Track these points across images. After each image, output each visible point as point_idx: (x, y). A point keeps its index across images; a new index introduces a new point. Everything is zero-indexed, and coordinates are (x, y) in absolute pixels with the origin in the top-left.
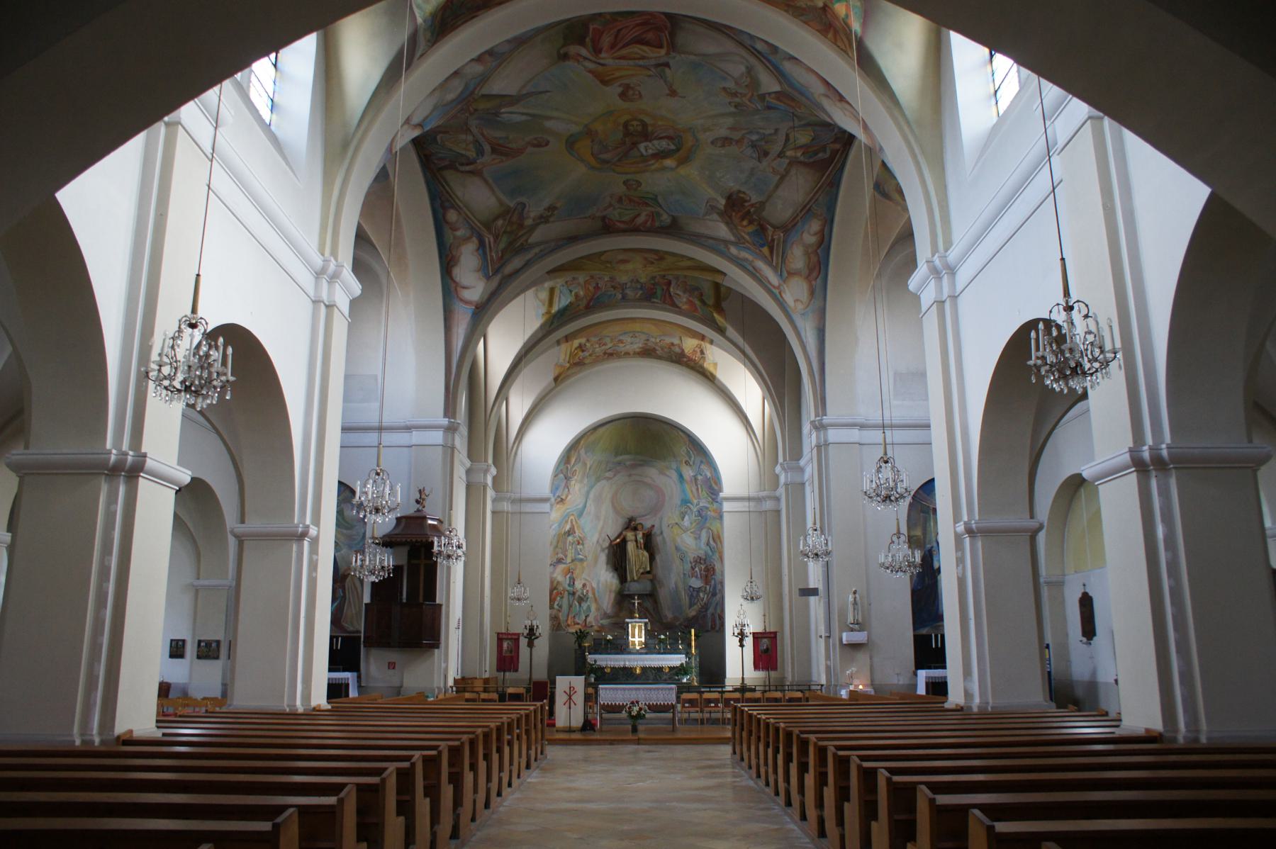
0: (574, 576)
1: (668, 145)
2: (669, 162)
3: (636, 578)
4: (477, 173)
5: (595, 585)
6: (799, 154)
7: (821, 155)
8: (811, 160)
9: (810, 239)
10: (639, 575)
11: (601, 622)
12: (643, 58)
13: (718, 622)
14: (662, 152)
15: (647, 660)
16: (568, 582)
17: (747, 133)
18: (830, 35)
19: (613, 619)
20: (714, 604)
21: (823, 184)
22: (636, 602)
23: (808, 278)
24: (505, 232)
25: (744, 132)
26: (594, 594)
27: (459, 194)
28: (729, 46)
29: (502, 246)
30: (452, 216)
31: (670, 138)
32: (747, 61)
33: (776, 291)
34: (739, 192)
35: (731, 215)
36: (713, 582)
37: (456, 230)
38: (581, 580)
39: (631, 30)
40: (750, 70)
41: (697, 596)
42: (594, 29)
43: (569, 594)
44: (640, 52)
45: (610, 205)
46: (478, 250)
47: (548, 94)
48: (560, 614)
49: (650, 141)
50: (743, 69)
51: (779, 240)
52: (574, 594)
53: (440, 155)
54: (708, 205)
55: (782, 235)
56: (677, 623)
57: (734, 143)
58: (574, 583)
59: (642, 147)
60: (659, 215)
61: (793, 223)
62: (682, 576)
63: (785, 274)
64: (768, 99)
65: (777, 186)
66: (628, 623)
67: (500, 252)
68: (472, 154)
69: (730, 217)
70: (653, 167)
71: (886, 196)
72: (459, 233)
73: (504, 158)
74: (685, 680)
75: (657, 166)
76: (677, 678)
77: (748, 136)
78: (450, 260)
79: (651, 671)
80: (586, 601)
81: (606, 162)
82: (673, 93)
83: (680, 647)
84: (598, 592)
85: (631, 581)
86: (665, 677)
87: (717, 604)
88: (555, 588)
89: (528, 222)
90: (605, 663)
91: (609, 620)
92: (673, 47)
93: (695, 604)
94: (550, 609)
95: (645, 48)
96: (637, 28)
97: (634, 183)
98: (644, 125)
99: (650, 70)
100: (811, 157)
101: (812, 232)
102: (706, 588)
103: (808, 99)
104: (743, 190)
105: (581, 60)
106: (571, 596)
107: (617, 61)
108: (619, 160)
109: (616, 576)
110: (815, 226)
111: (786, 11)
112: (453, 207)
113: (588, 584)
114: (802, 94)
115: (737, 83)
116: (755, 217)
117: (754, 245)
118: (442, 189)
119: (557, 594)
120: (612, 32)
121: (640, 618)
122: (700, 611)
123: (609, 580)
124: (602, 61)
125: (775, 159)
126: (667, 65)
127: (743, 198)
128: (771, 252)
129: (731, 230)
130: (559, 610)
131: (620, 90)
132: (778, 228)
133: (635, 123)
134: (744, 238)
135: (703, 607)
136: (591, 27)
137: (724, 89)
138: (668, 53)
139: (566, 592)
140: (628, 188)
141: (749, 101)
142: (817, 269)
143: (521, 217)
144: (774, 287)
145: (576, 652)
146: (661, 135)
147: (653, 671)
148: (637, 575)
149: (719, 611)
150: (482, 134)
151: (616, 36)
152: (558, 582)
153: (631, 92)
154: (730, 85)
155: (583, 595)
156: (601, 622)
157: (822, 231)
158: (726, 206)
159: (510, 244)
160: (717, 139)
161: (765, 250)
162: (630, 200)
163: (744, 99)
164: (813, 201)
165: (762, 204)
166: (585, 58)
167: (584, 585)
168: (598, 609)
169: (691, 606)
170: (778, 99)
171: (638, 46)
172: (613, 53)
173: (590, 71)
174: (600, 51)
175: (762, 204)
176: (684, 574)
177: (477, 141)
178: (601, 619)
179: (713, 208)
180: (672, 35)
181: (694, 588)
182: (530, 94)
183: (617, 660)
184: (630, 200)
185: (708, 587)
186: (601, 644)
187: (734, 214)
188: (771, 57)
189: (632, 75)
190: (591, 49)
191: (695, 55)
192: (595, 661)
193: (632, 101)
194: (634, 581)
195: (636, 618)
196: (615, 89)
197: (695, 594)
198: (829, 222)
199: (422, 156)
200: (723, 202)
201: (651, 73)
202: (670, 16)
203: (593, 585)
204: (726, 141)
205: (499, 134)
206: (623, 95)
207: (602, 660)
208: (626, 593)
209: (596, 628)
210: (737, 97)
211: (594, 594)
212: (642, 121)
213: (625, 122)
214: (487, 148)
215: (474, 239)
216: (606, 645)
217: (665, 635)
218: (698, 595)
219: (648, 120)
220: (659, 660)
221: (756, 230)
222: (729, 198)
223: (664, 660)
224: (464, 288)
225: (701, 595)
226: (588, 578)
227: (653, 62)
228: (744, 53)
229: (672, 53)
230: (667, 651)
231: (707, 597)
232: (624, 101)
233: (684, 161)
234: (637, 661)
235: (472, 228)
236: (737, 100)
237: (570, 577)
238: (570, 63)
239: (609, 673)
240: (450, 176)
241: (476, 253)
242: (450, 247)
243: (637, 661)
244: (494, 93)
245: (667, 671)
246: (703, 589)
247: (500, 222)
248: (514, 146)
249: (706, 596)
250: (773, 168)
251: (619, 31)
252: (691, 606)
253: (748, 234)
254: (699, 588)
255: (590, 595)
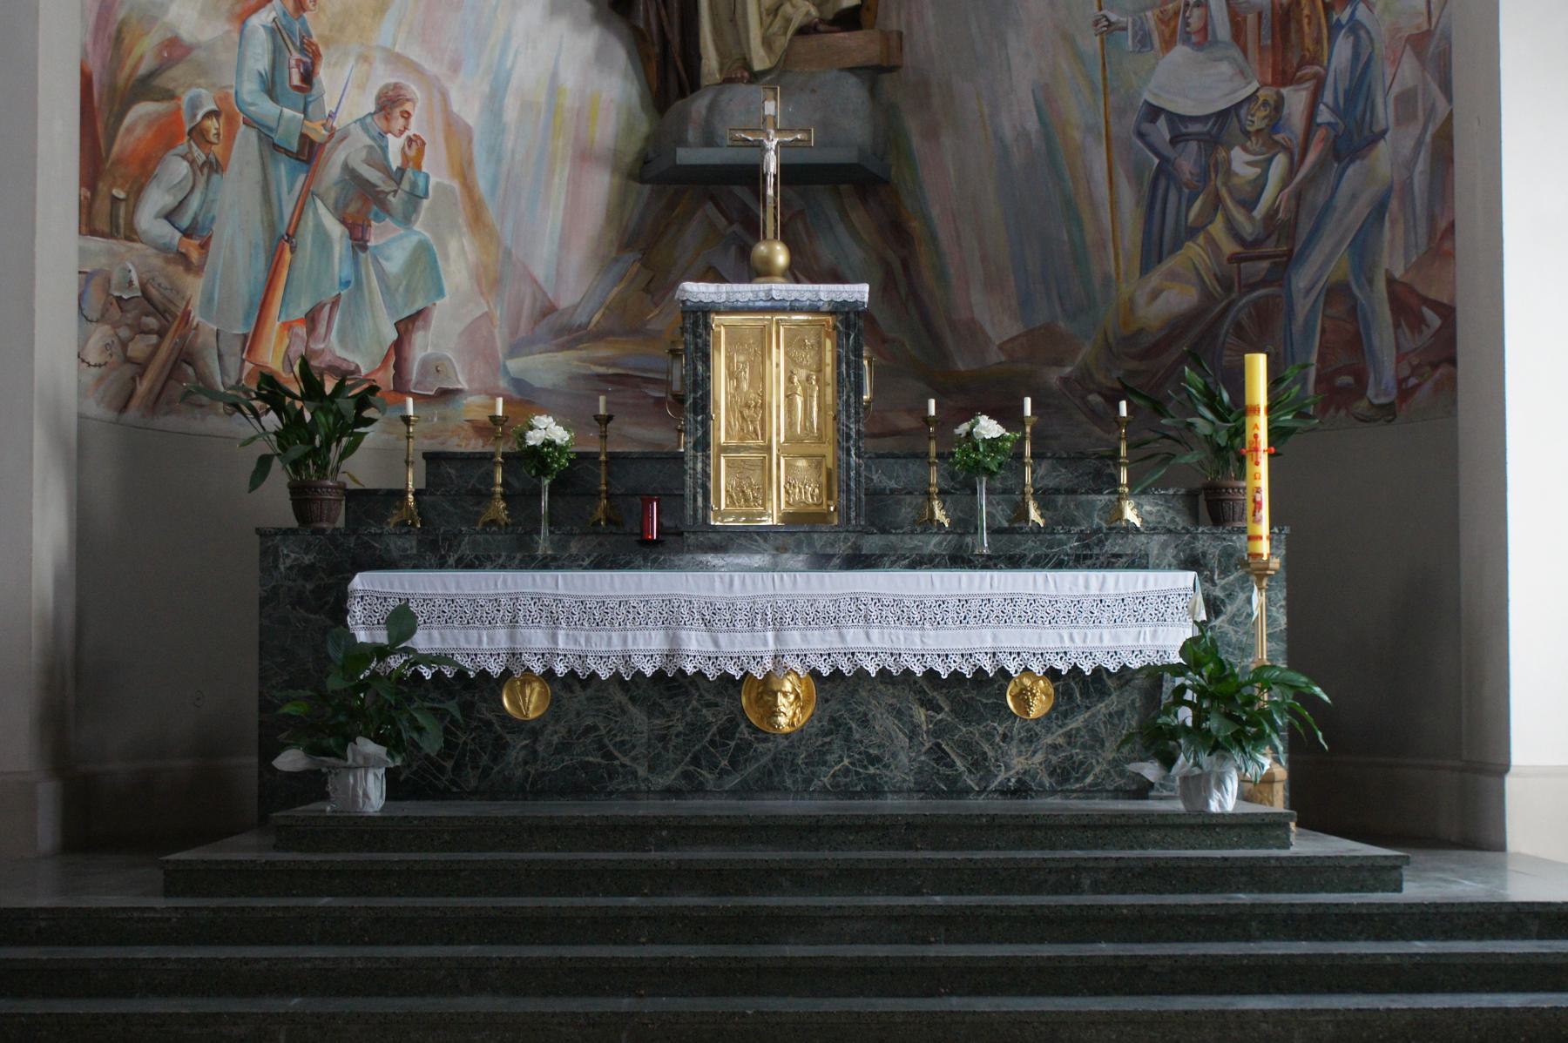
0: (317, 24)
3: (760, 60)
5: (469, 111)
10: (782, 43)
11: (514, 365)
13: (1384, 337)
15: (863, 612)
16: (259, 58)
19: (603, 352)
20: (1350, 215)
22: (772, 144)
26: (464, 172)
36: (1342, 51)
38: (364, 58)
41: (1204, 175)
43: (271, 146)
48: (195, 287)
52: (308, 153)
56: (1053, 377)
58: (308, 77)
62: (1091, 44)
66: (700, 315)
74: (1225, 800)
76: (1150, 771)
79: (899, 714)
80: (407, 220)
83: (1130, 514)
84: (495, 153)
85: (728, 80)
86: (1018, 762)
87: (1380, 209)
88: (144, 88)
90: (502, 639)
91: (561, 356)
93: (1192, 233)
94: (88, 226)
102: (1279, 103)
106: (283, 168)
109: (619, 54)
113: (414, 89)
119: (167, 135)
121: (796, 273)
122: (1226, 284)
123: (570, 79)
130: (183, 258)
135: (1249, 249)
139: (246, 143)
145: (269, 555)
147: (920, 715)
148: (767, 43)
149: (1394, 260)
152: (175, 50)
155: (385, 168)
156: (514, 365)
167: (390, 103)
168: (490, 280)
169: (1153, 252)
176: (1109, 29)
178: (514, 351)
181: (1175, 119)
183: (599, 615)
185: (1296, 100)
186: (484, 496)
192: (402, 620)
194: (755, 77)
195: (760, 272)
197: (1187, 162)
203: (455, 108)
207: (470, 614)
208: (688, 156)
209: (473, 407)
211: (464, 172)
216: (522, 499)
217: (1008, 415)
218: (1212, 167)
220: (967, 613)
223: (1030, 613)
225: (1241, 162)
226: (415, 53)
230: (1030, 546)
231: (1292, 170)
234: (779, 625)
237: (275, 31)
239: (533, 730)
243: (779, 625)
245: (1039, 706)
246: (1257, 119)
249: (1279, 164)
252: (1153, 252)
254: (1223, 116)
255: (436, 171)
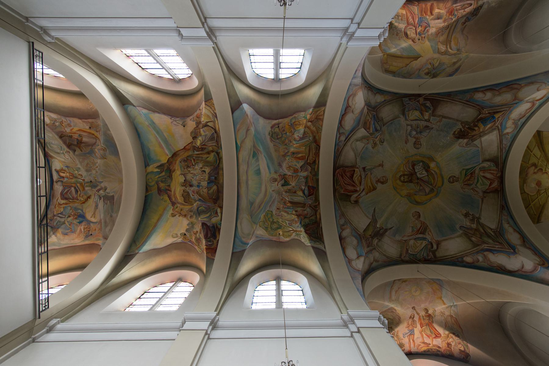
1: (420, 165)
2: (432, 165)
4: (438, 244)
6: (427, 113)
7: (428, 105)
8: (432, 108)
9: (489, 95)
12: (361, 176)
14: (424, 168)
17: (411, 136)
18: (186, 123)
21: (450, 99)
23: (519, 90)
24: (481, 238)
25: (409, 137)
27: (452, 253)
28: (348, 148)
29: (490, 241)
30: (468, 259)
31: (413, 166)
32: (353, 142)
33: (538, 103)
34: (454, 134)
35: (470, 135)
37: (479, 260)
39: (345, 180)
40: (357, 140)
42: (343, 192)
44: (357, 177)
45: (472, 189)
46: (494, 254)
47: (376, 209)
49: (416, 173)
50: (358, 143)
51: (489, 110)
53: (425, 255)
54: (465, 146)
55: (485, 110)
57: (419, 140)
59: (419, 176)
60: (484, 167)
61: (477, 106)
63: (517, 101)
64: (371, 132)
65: (450, 118)
67: (496, 243)
68: (424, 243)
69: (473, 136)
70: (437, 171)
71: (457, 70)
72: (481, 259)
73: (428, 230)
75: (436, 170)
77: (412, 136)
78: (501, 269)
81: (432, 190)
82: (381, 165)
89: (474, 226)
92: (353, 167)
95: (355, 175)
96: (344, 178)
97: (451, 179)
98: (404, 175)
99: (367, 174)
100: (430, 108)
101: (484, 95)
103: (360, 118)
104: (452, 133)
105: (359, 196)
107: (362, 185)
108: (431, 185)
110: (479, 96)
111: (321, 133)
112: (462, 258)
114: (360, 121)
115: (368, 144)
116: (472, 125)
117: (495, 121)
118: (449, 259)
120: (345, 186)
124: (361, 190)
125: (431, 123)
126: (364, 168)
127: (458, 132)
128: (498, 112)
129: (485, 134)
131: (379, 184)
132: (480, 112)
133: (402, 178)
134: (491, 127)
136: (343, 192)
137: (373, 148)
138: (358, 168)
140: (457, 182)
141: (377, 138)
142: (511, 86)
143: (471, 229)
144: (533, 105)
146: (411, 168)
150: (409, 236)
151: (348, 185)
153: (382, 180)
154: (370, 146)
157: (482, 91)
158: (465, 139)
159: (489, 236)
160: (415, 148)
161: (497, 116)
162: (469, 180)
163: (376, 140)
164: (461, 101)
165: (462, 123)
166: (359, 195)
170: (369, 128)
171: (354, 178)
172: (357, 186)
173: (367, 194)
174: (357, 190)
175: (462, 123)
177: (415, 239)
179: (467, 144)
180: (347, 167)
182: (373, 215)
184: (469, 180)
187: (469, 134)
188: (347, 134)
189: (371, 180)
190: (354, 193)
191: (356, 159)
193: (387, 180)
196: (379, 186)
198: (476, 90)
199: (424, 262)
200: (461, 140)
201: (369, 173)
202: (335, 169)
204: (417, 144)
205: (409, 230)
206: (382, 183)
210: (376, 143)
212: (401, 176)
213: (402, 182)
214: (421, 236)
215: (486, 253)
219: (401, 173)
221: (481, 122)
222: (458, 138)
224: (523, 267)
227: (363, 173)
228: (349, 144)
229: (357, 167)
232: (387, 182)
233: (432, 159)
235: (478, 253)
236: (378, 142)
238: (360, 200)
240: (439, 254)
241: (496, 255)
242: (488, 265)
244: (365, 228)
247: (473, 239)
248: (419, 226)
250: (437, 122)
251: (345, 184)
253: (485, 125)
